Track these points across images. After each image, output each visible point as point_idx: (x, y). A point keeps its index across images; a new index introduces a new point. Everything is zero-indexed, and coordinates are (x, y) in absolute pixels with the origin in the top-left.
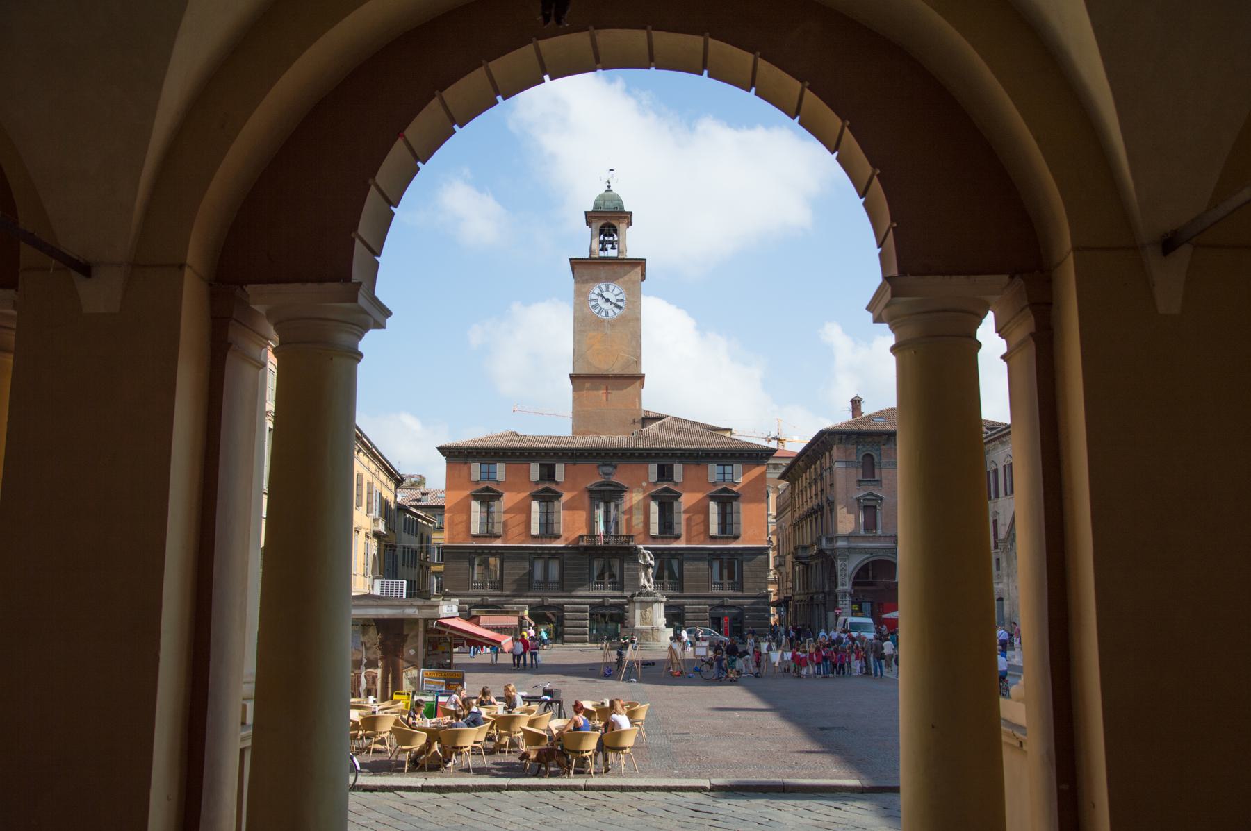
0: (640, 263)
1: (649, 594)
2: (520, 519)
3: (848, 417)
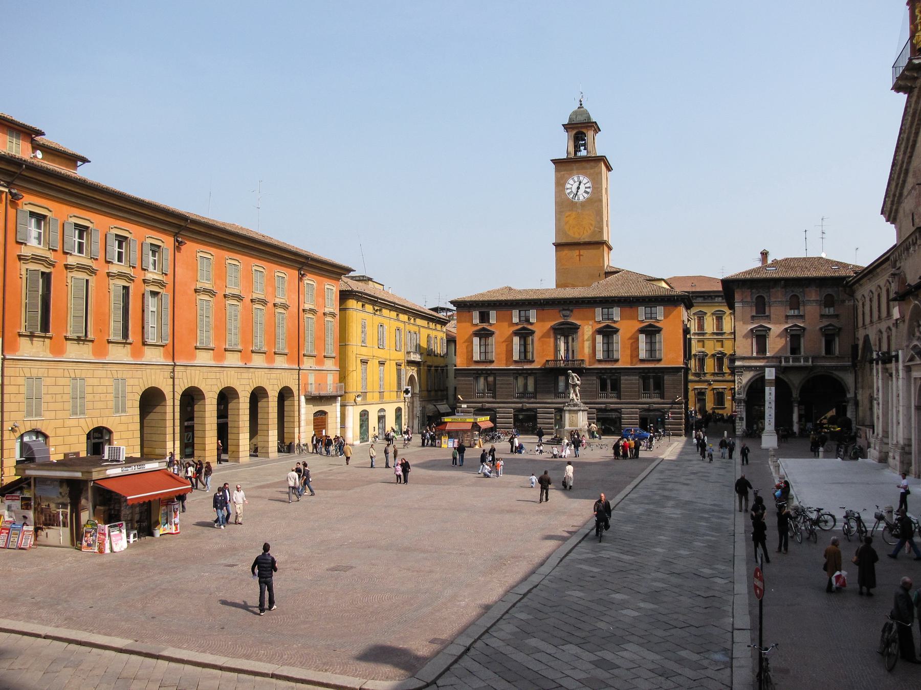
0: (602, 159)
1: (575, 405)
2: (502, 350)
3: (760, 264)
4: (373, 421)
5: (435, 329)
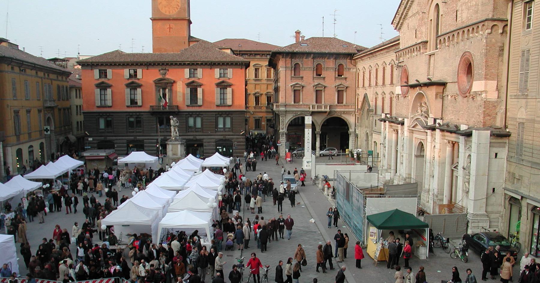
3: (293, 41)
4: (26, 155)
5: (62, 81)
